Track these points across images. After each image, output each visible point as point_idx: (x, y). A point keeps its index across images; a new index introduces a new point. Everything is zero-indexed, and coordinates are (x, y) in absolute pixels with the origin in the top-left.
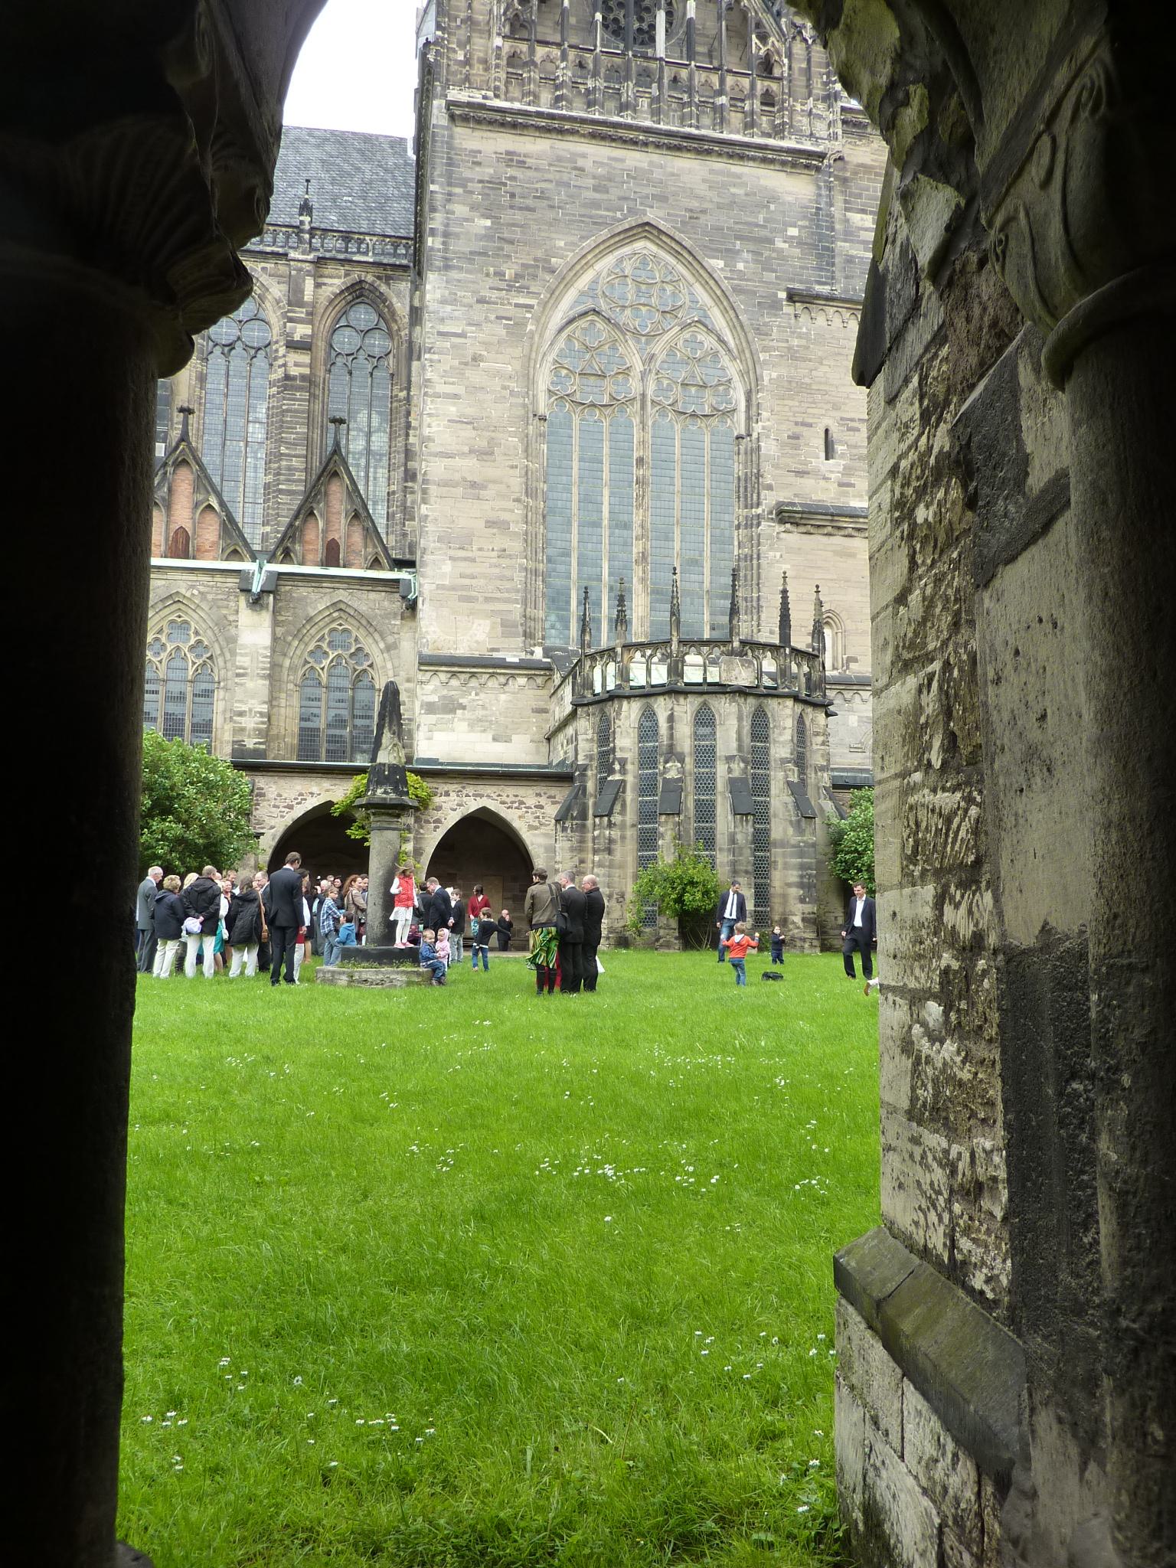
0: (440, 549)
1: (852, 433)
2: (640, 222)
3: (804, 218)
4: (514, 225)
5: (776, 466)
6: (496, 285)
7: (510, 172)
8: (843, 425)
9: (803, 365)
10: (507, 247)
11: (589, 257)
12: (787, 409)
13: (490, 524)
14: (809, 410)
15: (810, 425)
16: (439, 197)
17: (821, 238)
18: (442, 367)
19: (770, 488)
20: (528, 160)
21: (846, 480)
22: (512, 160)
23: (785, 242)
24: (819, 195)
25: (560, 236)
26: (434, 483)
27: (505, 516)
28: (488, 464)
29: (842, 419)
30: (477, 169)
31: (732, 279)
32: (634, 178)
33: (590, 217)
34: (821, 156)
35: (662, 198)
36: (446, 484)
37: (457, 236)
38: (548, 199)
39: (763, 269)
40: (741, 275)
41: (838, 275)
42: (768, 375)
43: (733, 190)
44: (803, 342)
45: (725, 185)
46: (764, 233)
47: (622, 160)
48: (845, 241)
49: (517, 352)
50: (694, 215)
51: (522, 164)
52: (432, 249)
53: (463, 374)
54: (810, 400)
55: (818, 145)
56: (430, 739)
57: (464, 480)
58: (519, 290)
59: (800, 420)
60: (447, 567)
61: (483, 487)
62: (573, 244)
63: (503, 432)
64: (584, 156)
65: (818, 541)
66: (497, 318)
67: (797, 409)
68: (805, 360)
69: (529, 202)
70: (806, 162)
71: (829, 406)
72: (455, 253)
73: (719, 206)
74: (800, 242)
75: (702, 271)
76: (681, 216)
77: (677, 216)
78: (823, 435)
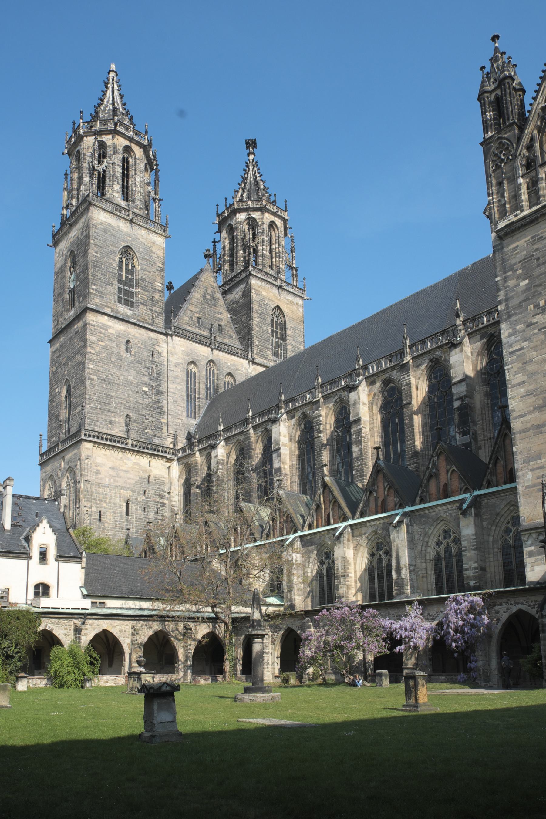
0: (525, 466)
26: (518, 433)
60: (530, 475)
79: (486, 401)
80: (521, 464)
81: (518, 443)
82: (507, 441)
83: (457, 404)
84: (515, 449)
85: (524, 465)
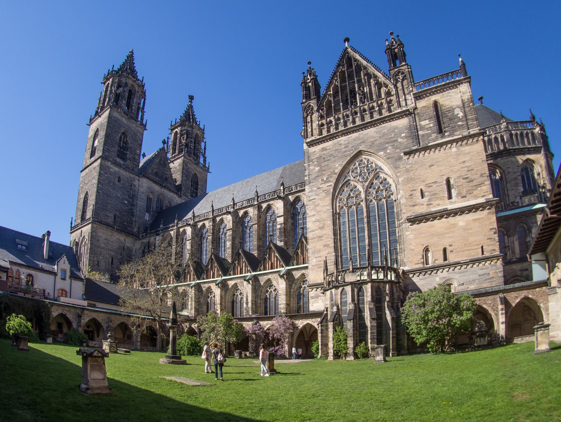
3: (406, 129)
5: (406, 206)
7: (323, 153)
9: (411, 172)
10: (324, 172)
13: (324, 246)
15: (416, 190)
16: (306, 167)
18: (310, 209)
19: (404, 213)
24: (410, 121)
27: (328, 243)
35: (364, 142)
36: (313, 239)
40: (389, 154)
43: (383, 131)
44: (411, 166)
45: (381, 131)
46: (395, 139)
47: (351, 137)
50: (373, 143)
58: (328, 182)
61: (322, 237)
64: (341, 140)
69: (328, 158)
71: (421, 182)
73: (380, 137)
74: (406, 137)
78: (420, 191)
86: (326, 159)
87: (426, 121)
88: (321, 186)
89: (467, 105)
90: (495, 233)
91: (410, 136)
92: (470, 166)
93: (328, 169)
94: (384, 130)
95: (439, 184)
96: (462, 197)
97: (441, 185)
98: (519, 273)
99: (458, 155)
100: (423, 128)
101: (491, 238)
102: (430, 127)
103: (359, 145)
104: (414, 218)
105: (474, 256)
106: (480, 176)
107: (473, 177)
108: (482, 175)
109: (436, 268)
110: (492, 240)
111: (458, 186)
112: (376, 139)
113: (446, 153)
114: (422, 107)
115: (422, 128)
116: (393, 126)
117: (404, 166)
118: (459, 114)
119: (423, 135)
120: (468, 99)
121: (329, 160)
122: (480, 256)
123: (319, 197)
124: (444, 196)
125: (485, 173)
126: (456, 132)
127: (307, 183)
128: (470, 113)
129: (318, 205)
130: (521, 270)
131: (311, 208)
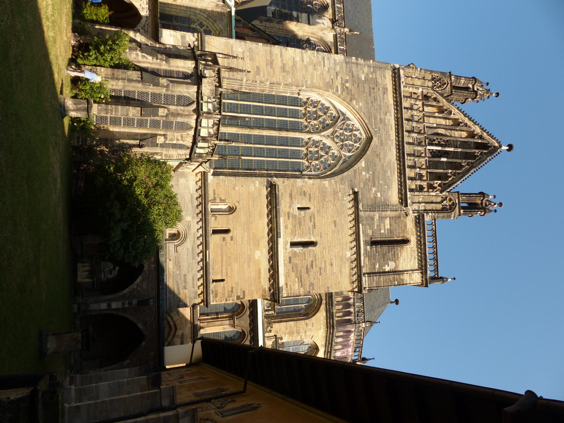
0: (247, 48)
1: (309, 218)
2: (373, 135)
3: (384, 199)
4: (364, 88)
5: (292, 186)
6: (343, 80)
7: (381, 89)
8: (312, 214)
9: (332, 198)
10: (356, 85)
11: (358, 115)
12: (315, 191)
13: (258, 68)
14: (315, 200)
15: (310, 201)
16: (369, 63)
17: (379, 206)
18: (312, 56)
19: (284, 182)
20: (386, 95)
21: (291, 215)
22: (385, 89)
23: (375, 191)
25: (363, 104)
26: (270, 49)
27: (262, 74)
28: (280, 70)
29: (314, 214)
30: (380, 77)
31: (359, 170)
32: (387, 133)
33: (371, 116)
34: (406, 206)
35: (382, 144)
37: (357, 67)
38: (375, 101)
39: (364, 182)
40: (360, 174)
41: (367, 213)
42: (326, 182)
43: (389, 171)
45: (390, 168)
46: (377, 185)
48: (379, 217)
49: (321, 85)
50: (378, 155)
51: (384, 93)
52: (352, 58)
53: (311, 64)
54: (320, 200)
55: (410, 205)
56: (171, 36)
57: (273, 60)
58: (342, 88)
59: (312, 196)
60: (240, 50)
61: (271, 67)
62: (361, 109)
63: (292, 77)
64: (391, 116)
65: (265, 202)
66: (332, 79)
67: (315, 194)
68: (334, 198)
69: (372, 95)
70: (403, 200)
71: (318, 208)
72: (351, 66)
73: (383, 165)
74: (376, 198)
75: (359, 158)
76: (377, 151)
77: (377, 149)
79: (291, 34)
80: (249, 46)
81: (264, 47)
82: (264, 41)
83: (295, 14)
84: (261, 44)
85: (248, 48)
86: (372, 90)
87: (389, 225)
88: (339, 78)
89: (397, 277)
90: (238, 297)
91: (375, 203)
92: (325, 271)
93: (359, 92)
94: (391, 172)
95: (311, 230)
96: (290, 258)
97: (310, 234)
98: (179, 333)
99: (341, 258)
100: (382, 220)
101: (232, 292)
102: (380, 229)
103: (380, 138)
104: (276, 193)
105: (213, 269)
106: (311, 283)
107: (311, 273)
108: (312, 285)
109: (205, 221)
110: (230, 293)
111: (305, 254)
112: (382, 161)
113: (346, 243)
114: (406, 223)
115: (382, 219)
116: (392, 185)
117: (342, 190)
118: (388, 266)
119: (373, 219)
120: (402, 280)
121: (370, 94)
122: (212, 277)
123: (325, 72)
124: (295, 235)
125: (313, 289)
126: (369, 259)
127: (347, 60)
128: (386, 279)
129: (315, 69)
130: (182, 334)
131: (313, 58)
